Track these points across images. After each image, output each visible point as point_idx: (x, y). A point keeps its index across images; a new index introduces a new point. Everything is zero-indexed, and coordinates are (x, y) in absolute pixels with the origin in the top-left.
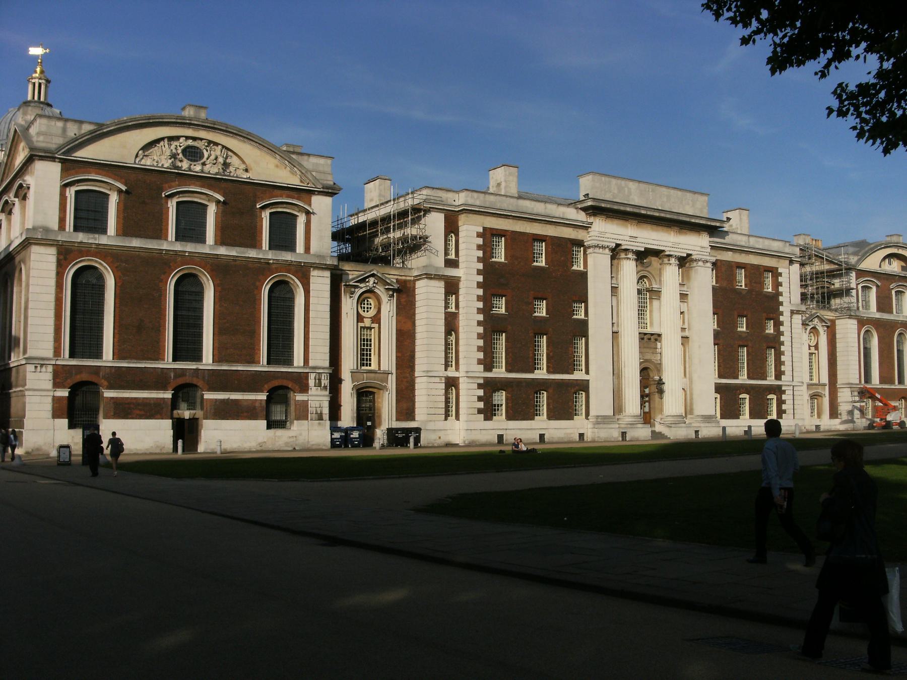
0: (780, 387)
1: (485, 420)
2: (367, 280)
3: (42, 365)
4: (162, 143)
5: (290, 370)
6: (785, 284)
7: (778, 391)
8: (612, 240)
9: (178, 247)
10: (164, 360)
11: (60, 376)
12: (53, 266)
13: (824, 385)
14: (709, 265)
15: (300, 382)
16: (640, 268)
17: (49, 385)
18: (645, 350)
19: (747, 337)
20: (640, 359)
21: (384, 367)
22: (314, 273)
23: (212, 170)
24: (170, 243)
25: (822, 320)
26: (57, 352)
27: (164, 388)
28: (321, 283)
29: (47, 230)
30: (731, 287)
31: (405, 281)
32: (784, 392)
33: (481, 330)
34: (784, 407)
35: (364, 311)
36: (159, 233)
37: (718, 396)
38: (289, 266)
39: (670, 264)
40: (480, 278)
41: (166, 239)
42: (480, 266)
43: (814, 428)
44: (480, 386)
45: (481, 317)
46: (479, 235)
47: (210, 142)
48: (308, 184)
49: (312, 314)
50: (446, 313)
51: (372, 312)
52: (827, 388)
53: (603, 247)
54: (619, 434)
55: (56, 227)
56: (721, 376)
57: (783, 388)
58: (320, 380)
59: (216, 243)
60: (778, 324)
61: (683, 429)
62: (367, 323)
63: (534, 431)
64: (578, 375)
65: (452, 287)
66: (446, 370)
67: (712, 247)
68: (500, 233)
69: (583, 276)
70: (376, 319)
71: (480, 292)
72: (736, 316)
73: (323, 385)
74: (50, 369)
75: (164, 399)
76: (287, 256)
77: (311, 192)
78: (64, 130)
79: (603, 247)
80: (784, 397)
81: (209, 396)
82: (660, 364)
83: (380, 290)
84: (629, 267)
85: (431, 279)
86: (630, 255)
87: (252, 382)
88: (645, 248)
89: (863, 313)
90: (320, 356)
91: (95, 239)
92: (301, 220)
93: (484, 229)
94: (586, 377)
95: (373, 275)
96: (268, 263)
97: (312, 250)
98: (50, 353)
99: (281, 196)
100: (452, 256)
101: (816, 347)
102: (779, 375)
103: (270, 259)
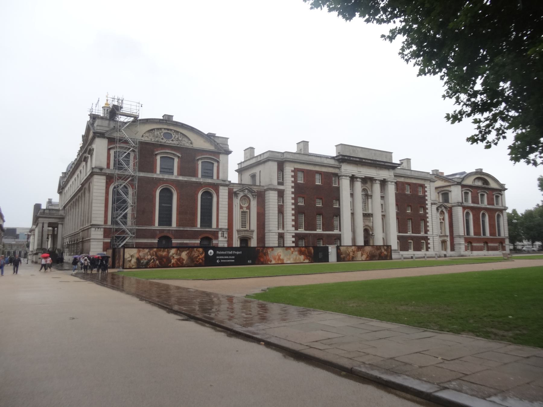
0: (427, 237)
2: (244, 191)
3: (98, 228)
4: (154, 131)
5: (210, 230)
6: (428, 192)
7: (426, 239)
8: (350, 173)
9: (161, 176)
10: (154, 225)
11: (107, 233)
12: (104, 184)
13: (447, 236)
14: (393, 183)
15: (215, 234)
16: (363, 185)
17: (102, 237)
18: (365, 221)
20: (363, 225)
21: (252, 228)
22: (221, 188)
23: (176, 143)
24: (158, 174)
25: (445, 208)
26: (106, 222)
27: (153, 237)
28: (224, 192)
29: (101, 169)
31: (261, 191)
32: (429, 239)
33: (293, 212)
34: (429, 246)
35: (243, 204)
36: (153, 170)
37: (399, 241)
38: (210, 185)
39: (376, 183)
40: (293, 190)
41: (156, 172)
42: (293, 185)
43: (443, 255)
44: (293, 237)
45: (293, 207)
46: (292, 171)
47: (175, 131)
48: (218, 149)
49: (220, 206)
50: (278, 205)
51: (246, 205)
52: (449, 237)
53: (346, 176)
56: (399, 232)
58: (223, 234)
59: (178, 175)
60: (425, 209)
62: (245, 209)
64: (336, 232)
65: (281, 194)
66: (278, 230)
67: (395, 176)
68: (302, 171)
69: (338, 189)
70: (249, 208)
71: (293, 196)
73: (225, 236)
74: (102, 230)
75: (154, 243)
76: (209, 181)
77: (219, 153)
78: (109, 124)
79: (346, 176)
80: (429, 241)
81: (174, 241)
82: (373, 227)
83: (249, 195)
84: (358, 185)
86: (358, 180)
87: (194, 235)
88: (365, 176)
89: (465, 204)
90: (224, 224)
91: (123, 172)
92: (216, 164)
93: (295, 169)
94: (339, 233)
95: (246, 189)
96: (201, 184)
97: (220, 178)
98: (102, 223)
99: (206, 155)
100: (281, 181)
101: (443, 219)
102: (426, 231)
103: (202, 182)
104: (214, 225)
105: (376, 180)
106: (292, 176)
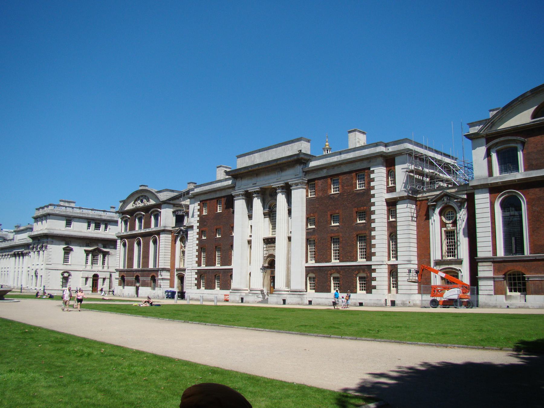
1: (197, 289)
7: (369, 269)
19: (338, 230)
30: (326, 195)
33: (197, 248)
54: (239, 299)
55: (120, 232)
57: (373, 267)
61: (275, 298)
63: (213, 295)
72: (329, 216)
79: (238, 195)
85: (190, 228)
97: (161, 226)
104: (157, 267)
105: (275, 189)
106: (199, 210)
